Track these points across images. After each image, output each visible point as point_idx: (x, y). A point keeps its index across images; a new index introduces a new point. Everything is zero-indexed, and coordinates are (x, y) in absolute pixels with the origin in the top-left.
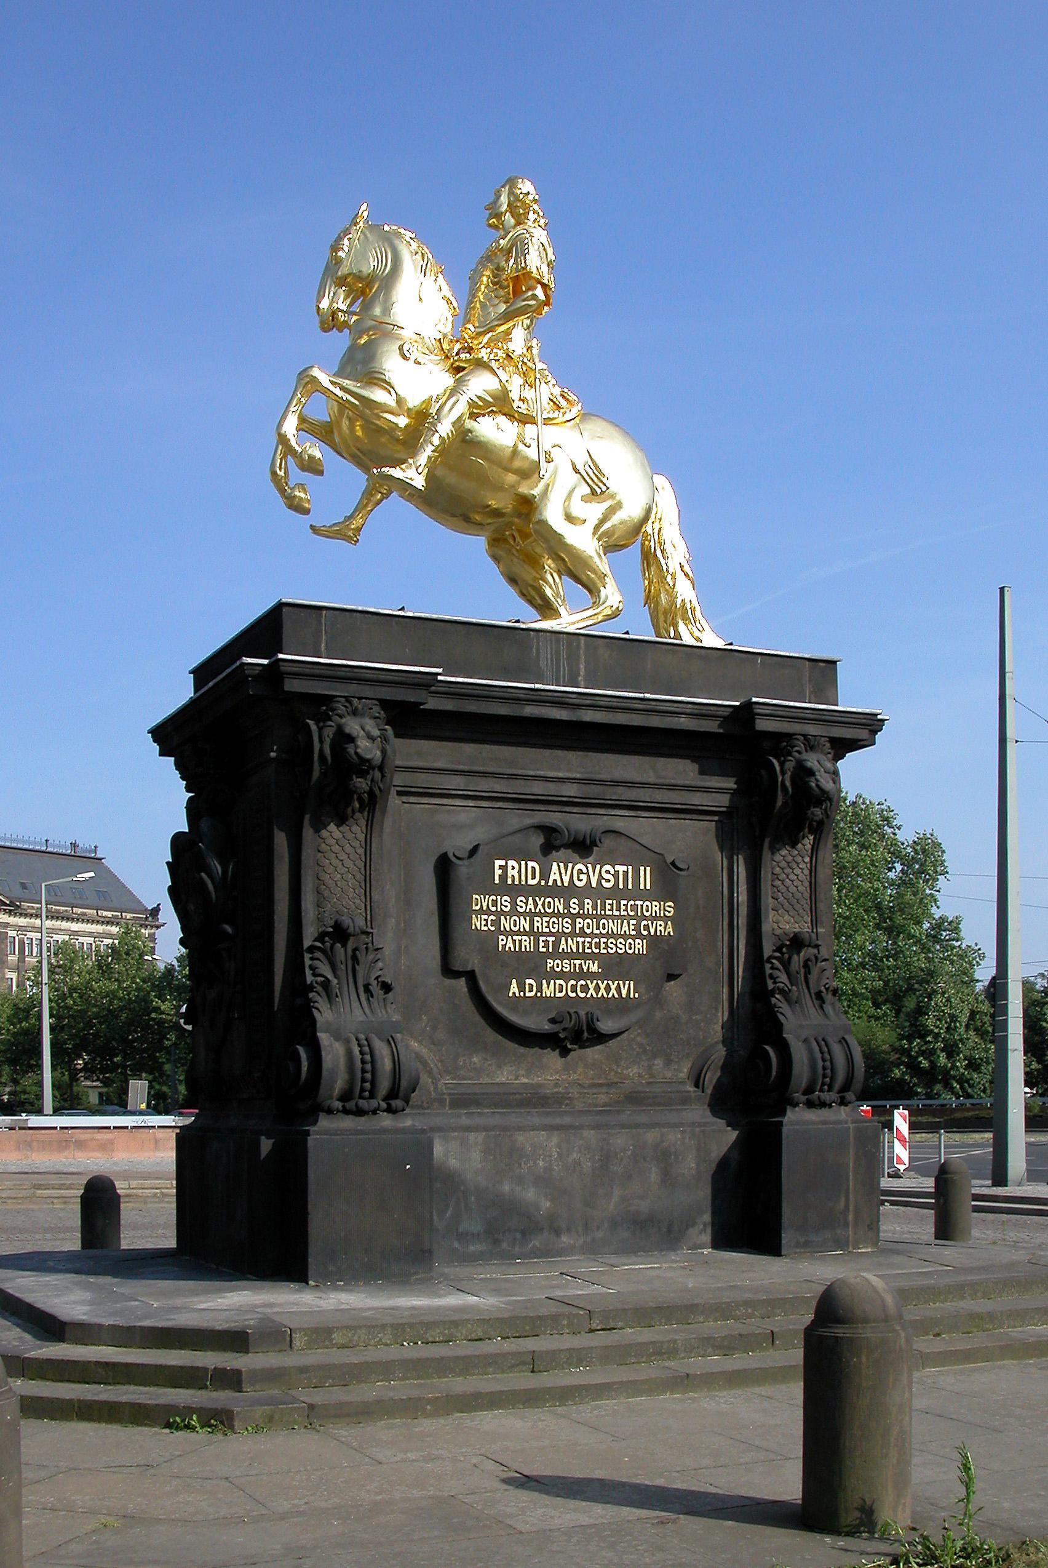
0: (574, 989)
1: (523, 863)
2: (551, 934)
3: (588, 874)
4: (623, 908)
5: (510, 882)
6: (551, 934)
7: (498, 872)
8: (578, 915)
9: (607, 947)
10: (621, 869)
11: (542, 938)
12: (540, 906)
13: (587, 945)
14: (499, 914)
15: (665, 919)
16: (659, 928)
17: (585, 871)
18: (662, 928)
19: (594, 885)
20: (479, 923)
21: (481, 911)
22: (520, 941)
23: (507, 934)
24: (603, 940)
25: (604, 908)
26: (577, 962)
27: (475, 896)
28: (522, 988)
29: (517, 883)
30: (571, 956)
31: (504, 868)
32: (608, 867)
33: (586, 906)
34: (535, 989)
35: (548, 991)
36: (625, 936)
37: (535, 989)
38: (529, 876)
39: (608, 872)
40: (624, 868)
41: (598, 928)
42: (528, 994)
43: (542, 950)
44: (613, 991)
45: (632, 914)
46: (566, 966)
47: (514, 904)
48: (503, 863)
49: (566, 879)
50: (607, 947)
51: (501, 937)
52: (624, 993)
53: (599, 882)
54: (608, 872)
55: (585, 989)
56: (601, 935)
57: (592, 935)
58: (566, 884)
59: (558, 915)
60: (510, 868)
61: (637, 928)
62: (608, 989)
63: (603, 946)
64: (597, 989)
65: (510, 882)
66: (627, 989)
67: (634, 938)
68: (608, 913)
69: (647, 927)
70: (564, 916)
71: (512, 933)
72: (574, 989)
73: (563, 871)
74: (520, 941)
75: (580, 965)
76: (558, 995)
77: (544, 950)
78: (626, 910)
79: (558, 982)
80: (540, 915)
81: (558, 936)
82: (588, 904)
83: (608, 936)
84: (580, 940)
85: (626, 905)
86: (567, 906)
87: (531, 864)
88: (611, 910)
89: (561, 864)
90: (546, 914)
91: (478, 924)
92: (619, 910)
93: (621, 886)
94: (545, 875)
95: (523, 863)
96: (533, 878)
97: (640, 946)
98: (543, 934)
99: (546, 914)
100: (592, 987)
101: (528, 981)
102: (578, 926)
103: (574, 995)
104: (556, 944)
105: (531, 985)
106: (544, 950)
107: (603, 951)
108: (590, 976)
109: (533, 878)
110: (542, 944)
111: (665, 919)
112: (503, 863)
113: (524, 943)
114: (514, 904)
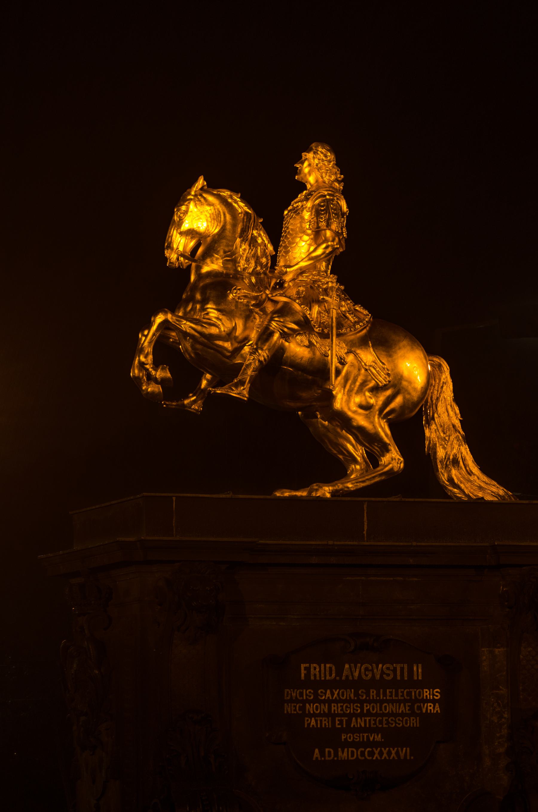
0: (363, 754)
1: (322, 665)
2: (344, 715)
3: (372, 670)
4: (400, 694)
5: (312, 678)
6: (344, 715)
7: (303, 672)
8: (365, 701)
9: (388, 723)
10: (398, 667)
11: (337, 718)
12: (336, 695)
13: (373, 722)
14: (304, 702)
15: (434, 701)
16: (429, 708)
17: (370, 668)
18: (431, 708)
19: (378, 677)
20: (289, 709)
21: (291, 701)
22: (321, 721)
23: (311, 716)
24: (384, 719)
25: (385, 694)
26: (365, 735)
27: (286, 690)
28: (322, 753)
29: (318, 678)
30: (360, 730)
31: (308, 669)
32: (388, 665)
33: (371, 694)
34: (332, 755)
35: (344, 755)
36: (403, 715)
37: (332, 755)
38: (327, 673)
39: (388, 668)
40: (402, 665)
41: (381, 709)
42: (327, 758)
43: (337, 726)
44: (393, 754)
45: (409, 698)
46: (357, 738)
47: (316, 695)
48: (307, 665)
49: (356, 674)
50: (388, 723)
51: (307, 719)
52: (402, 755)
53: (381, 676)
54: (388, 668)
55: (372, 754)
56: (383, 715)
57: (377, 715)
58: (356, 678)
59: (350, 701)
60: (312, 670)
61: (412, 708)
62: (389, 753)
63: (384, 722)
64: (381, 754)
65: (312, 678)
66: (405, 752)
67: (409, 715)
68: (388, 698)
69: (420, 708)
70: (354, 702)
71: (314, 715)
72: (363, 754)
73: (353, 669)
74: (321, 721)
75: (367, 736)
76: (350, 758)
77: (340, 726)
78: (403, 696)
79: (350, 749)
80: (336, 701)
81: (350, 716)
82: (373, 693)
83: (389, 715)
84: (368, 719)
85: (403, 692)
86: (356, 694)
87: (328, 665)
88: (391, 696)
89: (352, 665)
90: (340, 701)
91: (289, 710)
92: (397, 695)
93: (399, 678)
94: (339, 672)
95: (322, 665)
96: (331, 675)
97: (414, 722)
98: (338, 715)
99: (340, 701)
100: (377, 752)
101: (327, 750)
102: (365, 709)
103: (363, 758)
104: (349, 722)
105: (329, 752)
106: (340, 726)
107: (385, 726)
108: (375, 744)
109: (331, 675)
110: (337, 722)
111: (434, 701)
112: (307, 665)
113: (323, 723)
114: (316, 695)
